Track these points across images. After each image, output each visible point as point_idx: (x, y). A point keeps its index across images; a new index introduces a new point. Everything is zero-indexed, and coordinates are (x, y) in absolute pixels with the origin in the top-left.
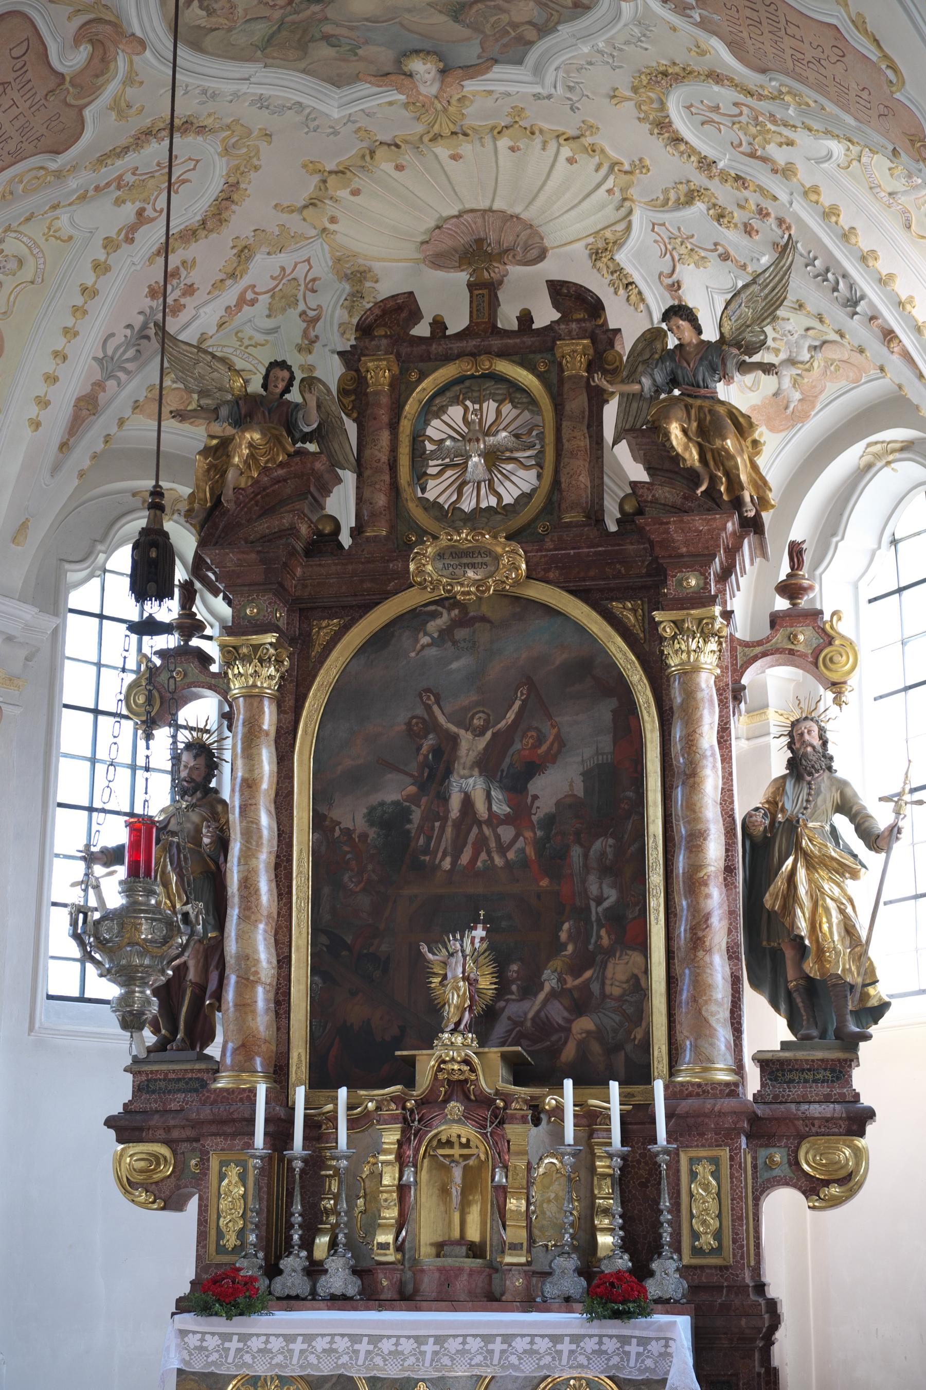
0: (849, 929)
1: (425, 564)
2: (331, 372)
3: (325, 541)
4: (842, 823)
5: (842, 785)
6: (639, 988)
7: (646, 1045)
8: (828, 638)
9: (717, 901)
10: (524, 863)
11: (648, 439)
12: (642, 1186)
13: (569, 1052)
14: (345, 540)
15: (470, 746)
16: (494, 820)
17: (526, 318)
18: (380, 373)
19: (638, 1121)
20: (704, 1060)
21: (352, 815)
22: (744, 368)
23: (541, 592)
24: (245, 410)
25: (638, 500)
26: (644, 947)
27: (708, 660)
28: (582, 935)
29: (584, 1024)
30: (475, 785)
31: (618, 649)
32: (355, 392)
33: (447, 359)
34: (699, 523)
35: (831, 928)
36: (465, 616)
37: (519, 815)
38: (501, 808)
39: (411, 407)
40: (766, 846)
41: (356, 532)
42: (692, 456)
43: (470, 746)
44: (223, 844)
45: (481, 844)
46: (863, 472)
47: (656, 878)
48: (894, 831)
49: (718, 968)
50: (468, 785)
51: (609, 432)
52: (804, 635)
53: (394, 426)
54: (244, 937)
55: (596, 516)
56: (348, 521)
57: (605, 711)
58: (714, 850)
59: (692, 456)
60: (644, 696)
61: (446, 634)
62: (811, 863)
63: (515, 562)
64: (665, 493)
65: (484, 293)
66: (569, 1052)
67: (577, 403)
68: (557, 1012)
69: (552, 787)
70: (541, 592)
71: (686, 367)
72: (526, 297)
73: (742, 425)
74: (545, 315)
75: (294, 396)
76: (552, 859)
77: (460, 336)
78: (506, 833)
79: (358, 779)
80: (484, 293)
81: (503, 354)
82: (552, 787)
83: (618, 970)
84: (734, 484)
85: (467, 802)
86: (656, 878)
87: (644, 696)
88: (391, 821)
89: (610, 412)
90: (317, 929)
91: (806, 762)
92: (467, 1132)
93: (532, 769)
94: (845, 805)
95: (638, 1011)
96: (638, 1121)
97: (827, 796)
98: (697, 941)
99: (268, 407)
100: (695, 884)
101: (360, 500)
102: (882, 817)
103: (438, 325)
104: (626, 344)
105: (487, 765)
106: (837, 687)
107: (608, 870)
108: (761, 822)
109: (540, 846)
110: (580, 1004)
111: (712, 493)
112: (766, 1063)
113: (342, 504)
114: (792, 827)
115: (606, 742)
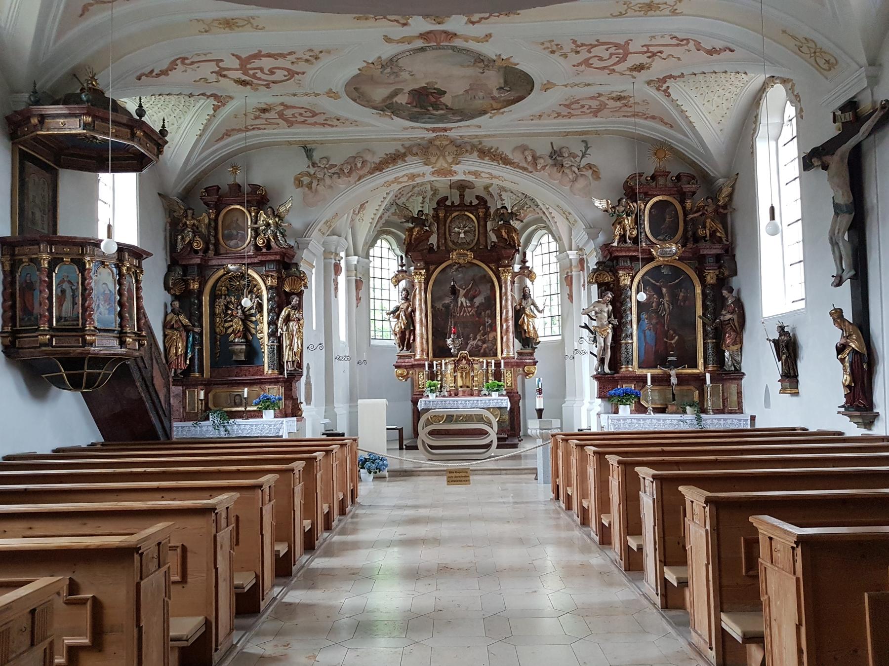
0: (534, 328)
1: (454, 255)
2: (432, 213)
3: (431, 249)
4: (532, 307)
5: (533, 300)
6: (495, 339)
7: (496, 349)
8: (531, 272)
9: (511, 323)
10: (473, 315)
11: (498, 232)
12: (498, 376)
13: (482, 351)
14: (435, 247)
15: (462, 292)
16: (467, 307)
17: (471, 202)
18: (441, 215)
19: (498, 365)
20: (508, 352)
21: (439, 305)
22: (517, 219)
23: (475, 261)
24: (413, 220)
25: (495, 245)
26: (496, 331)
27: (509, 278)
28: (484, 329)
29: (485, 345)
30: (463, 300)
31: (491, 273)
32: (436, 217)
33: (456, 211)
34: (508, 251)
35: (531, 328)
36: (461, 266)
37: (472, 306)
38: (469, 304)
39: (448, 221)
40: (519, 313)
41: (438, 247)
42: (506, 237)
43: (462, 292)
44: (414, 311)
45: (465, 311)
46: (535, 230)
47: (498, 318)
48: (543, 310)
49: (511, 335)
50: (462, 300)
51: (488, 229)
52: (527, 272)
53: (445, 225)
54: (421, 330)
55: (486, 247)
56: (435, 243)
57: (489, 285)
58: (510, 314)
59: (506, 237)
60: (496, 283)
61: (457, 269)
62: (527, 316)
63: (471, 255)
64: (501, 244)
65: (462, 196)
66: (482, 351)
67: (482, 223)
68: (480, 343)
69: (478, 301)
70: (475, 261)
71: (505, 217)
72: (470, 198)
73: (515, 230)
74: (475, 202)
75: (423, 217)
76: (478, 314)
77: (458, 206)
78: (470, 309)
79: (440, 298)
80: (462, 196)
81: (467, 211)
82: (478, 301)
83: (491, 335)
84: (514, 242)
85: (462, 303)
86: (498, 318)
87: (496, 283)
88: (447, 307)
89: (489, 223)
90: (433, 328)
91: (525, 295)
92: (467, 366)
93: (475, 297)
94: (533, 304)
95: (495, 344)
96: (498, 365)
97: (530, 302)
98: (507, 331)
99: (418, 220)
100: (507, 320)
101: (438, 241)
102: (541, 309)
103: (453, 203)
104: (492, 211)
105: (465, 296)
106: (532, 281)
107: (489, 317)
108: (518, 307)
109: (476, 312)
110: (484, 343)
111: (510, 244)
112: (518, 353)
113: (433, 240)
114: (524, 308)
115: (489, 292)
